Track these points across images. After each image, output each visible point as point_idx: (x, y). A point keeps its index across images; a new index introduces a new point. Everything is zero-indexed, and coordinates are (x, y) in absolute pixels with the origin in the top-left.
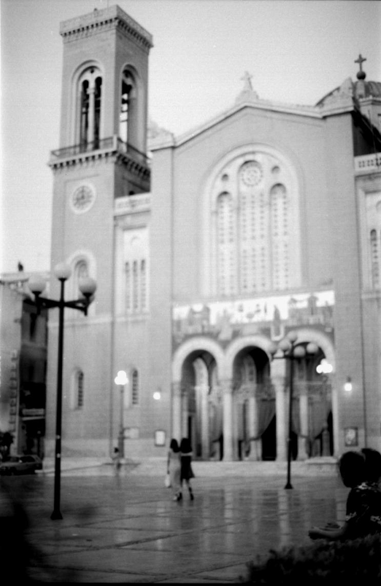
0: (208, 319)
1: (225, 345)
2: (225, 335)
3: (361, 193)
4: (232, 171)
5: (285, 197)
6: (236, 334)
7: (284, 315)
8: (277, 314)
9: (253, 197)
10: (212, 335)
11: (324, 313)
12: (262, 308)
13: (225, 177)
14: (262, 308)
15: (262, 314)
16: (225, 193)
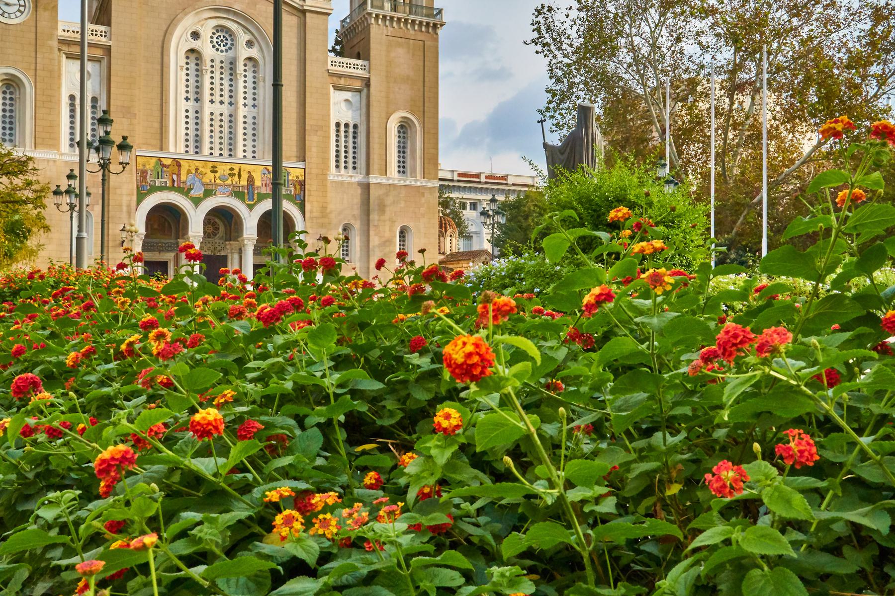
0: (179, 175)
1: (197, 202)
2: (198, 192)
3: (332, 89)
4: (207, 31)
5: (254, 72)
6: (208, 193)
7: (258, 183)
8: (251, 179)
9: (222, 62)
10: (185, 191)
11: (294, 185)
12: (236, 172)
13: (195, 35)
14: (236, 172)
15: (236, 178)
16: (192, 51)
